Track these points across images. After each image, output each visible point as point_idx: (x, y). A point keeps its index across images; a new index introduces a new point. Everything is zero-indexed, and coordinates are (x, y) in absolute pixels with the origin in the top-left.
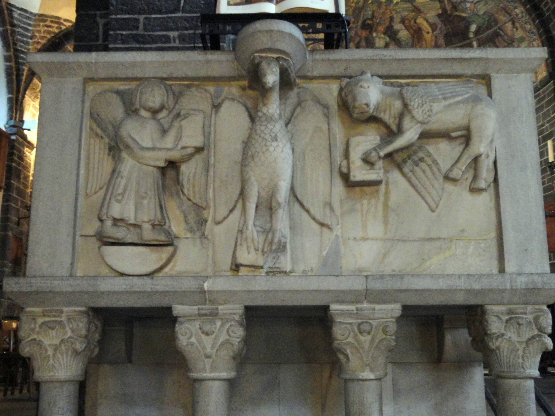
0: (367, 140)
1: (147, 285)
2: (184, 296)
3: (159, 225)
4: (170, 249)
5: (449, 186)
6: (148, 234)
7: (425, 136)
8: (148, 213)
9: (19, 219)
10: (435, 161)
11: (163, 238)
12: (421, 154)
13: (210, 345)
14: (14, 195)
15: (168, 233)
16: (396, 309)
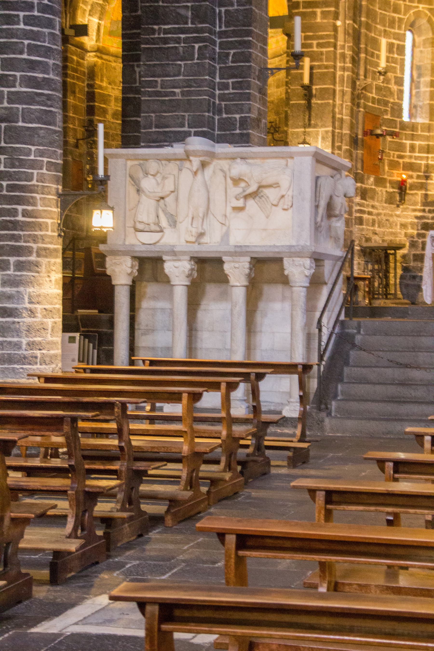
0: (238, 190)
1: (153, 248)
2: (167, 253)
3: (157, 224)
4: (161, 234)
5: (274, 208)
6: (153, 227)
7: (260, 187)
8: (152, 219)
9: (78, 140)
10: (268, 197)
11: (158, 229)
12: (262, 194)
13: (178, 271)
14: (71, 115)
15: (160, 227)
16: (248, 259)
